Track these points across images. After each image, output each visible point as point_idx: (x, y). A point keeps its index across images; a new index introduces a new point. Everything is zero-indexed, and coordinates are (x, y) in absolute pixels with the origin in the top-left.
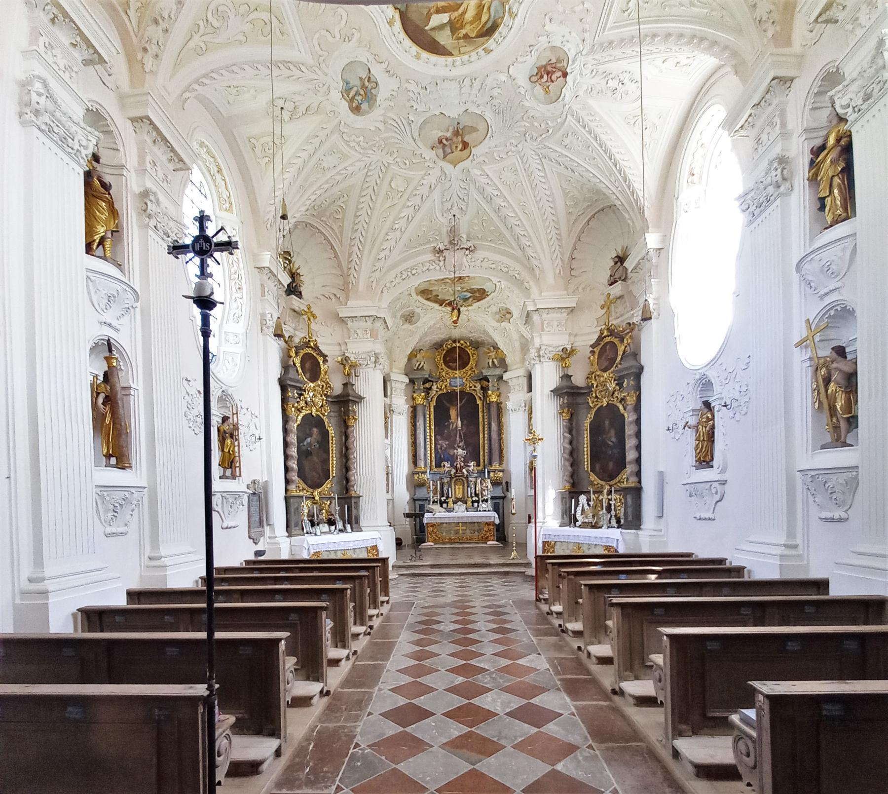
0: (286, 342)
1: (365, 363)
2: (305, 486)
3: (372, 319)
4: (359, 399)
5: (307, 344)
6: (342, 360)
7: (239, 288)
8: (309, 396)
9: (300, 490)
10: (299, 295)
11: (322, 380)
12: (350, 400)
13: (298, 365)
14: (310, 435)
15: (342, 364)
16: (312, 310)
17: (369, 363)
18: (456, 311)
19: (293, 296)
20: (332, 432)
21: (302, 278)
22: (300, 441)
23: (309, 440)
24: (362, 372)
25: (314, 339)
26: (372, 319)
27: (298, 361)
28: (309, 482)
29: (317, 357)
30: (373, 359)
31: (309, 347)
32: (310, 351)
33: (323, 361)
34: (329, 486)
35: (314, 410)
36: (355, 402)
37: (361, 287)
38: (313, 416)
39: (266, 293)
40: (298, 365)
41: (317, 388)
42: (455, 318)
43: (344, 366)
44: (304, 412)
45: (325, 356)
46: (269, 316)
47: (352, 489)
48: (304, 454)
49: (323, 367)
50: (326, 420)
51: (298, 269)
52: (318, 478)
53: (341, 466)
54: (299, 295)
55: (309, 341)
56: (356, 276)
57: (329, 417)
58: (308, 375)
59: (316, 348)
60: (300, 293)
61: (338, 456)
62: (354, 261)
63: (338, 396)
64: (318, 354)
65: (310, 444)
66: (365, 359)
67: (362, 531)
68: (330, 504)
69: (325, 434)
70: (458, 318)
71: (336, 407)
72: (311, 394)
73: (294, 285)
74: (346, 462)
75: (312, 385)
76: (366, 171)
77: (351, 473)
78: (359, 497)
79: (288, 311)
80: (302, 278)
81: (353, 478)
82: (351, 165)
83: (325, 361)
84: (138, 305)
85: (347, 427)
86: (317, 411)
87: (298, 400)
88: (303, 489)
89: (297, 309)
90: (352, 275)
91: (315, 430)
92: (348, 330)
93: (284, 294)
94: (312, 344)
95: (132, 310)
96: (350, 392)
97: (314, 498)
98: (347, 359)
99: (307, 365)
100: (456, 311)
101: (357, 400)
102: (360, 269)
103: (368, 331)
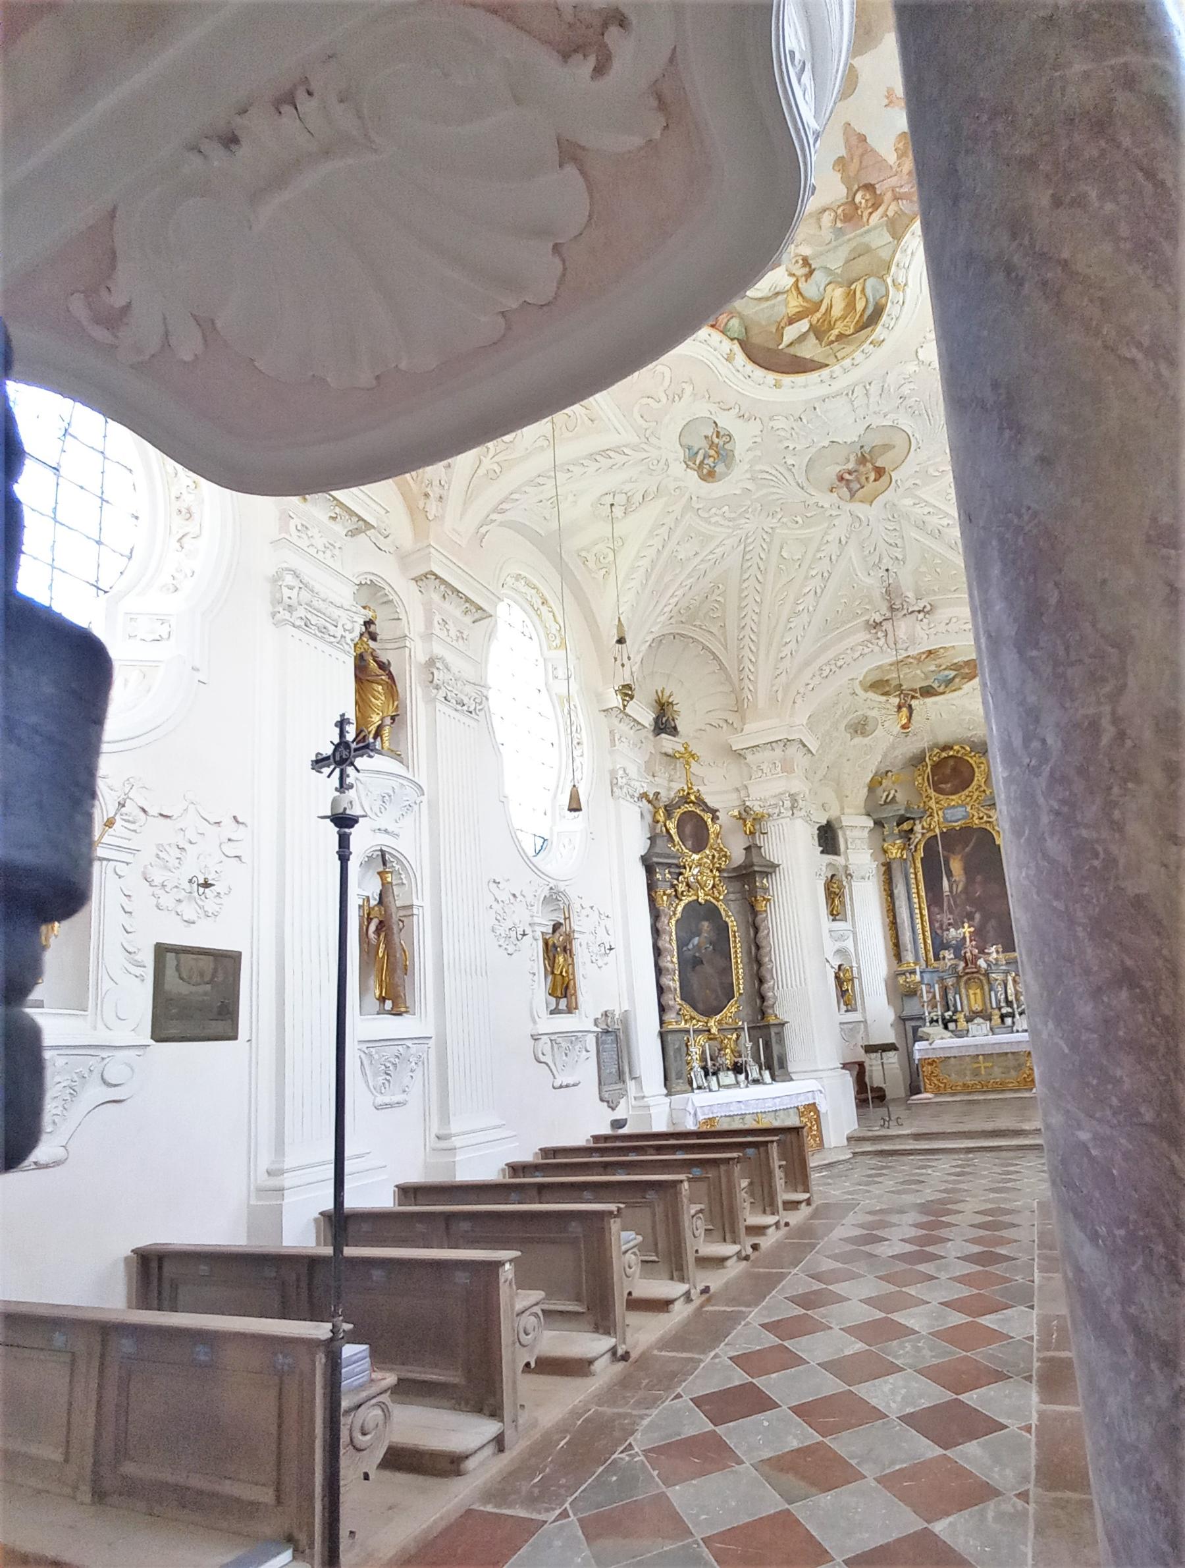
0: (649, 802)
1: (777, 811)
2: (694, 1014)
3: (781, 744)
4: (771, 869)
5: (685, 800)
6: (740, 813)
7: (578, 743)
8: (691, 874)
9: (686, 1021)
10: (674, 731)
11: (711, 848)
12: (755, 871)
13: (673, 831)
14: (699, 935)
15: (740, 818)
16: (690, 749)
17: (782, 811)
18: (904, 710)
19: (663, 735)
20: (732, 924)
21: (675, 708)
22: (682, 944)
23: (696, 940)
24: (771, 826)
25: (695, 788)
26: (781, 744)
27: (672, 826)
28: (700, 1006)
29: (702, 814)
30: (788, 804)
31: (688, 803)
32: (691, 808)
33: (712, 819)
34: (733, 1010)
35: (701, 893)
36: (766, 874)
37: (761, 703)
38: (700, 904)
39: (617, 742)
40: (673, 831)
41: (705, 860)
42: (904, 721)
43: (745, 820)
44: (686, 900)
45: (714, 812)
46: (621, 772)
47: (770, 1011)
48: (690, 964)
49: (713, 828)
50: (722, 907)
51: (670, 696)
52: (715, 999)
53: (751, 976)
54: (674, 731)
55: (688, 794)
56: (751, 688)
57: (726, 901)
58: (689, 843)
59: (700, 802)
60: (675, 728)
61: (746, 960)
62: (746, 669)
63: (734, 869)
64: (703, 810)
65: (698, 947)
66: (776, 806)
67: (792, 1080)
68: (738, 1038)
69: (722, 929)
70: (910, 718)
71: (737, 885)
72: (695, 871)
73: (664, 719)
74: (759, 969)
75: (696, 857)
76: (743, 546)
77: (766, 986)
78: (783, 1024)
79: (658, 756)
80: (675, 708)
81: (770, 994)
82: (720, 545)
83: (715, 818)
84: (424, 799)
85: (755, 913)
86: (706, 895)
87: (675, 882)
88: (692, 1018)
89: (670, 752)
90: (746, 690)
91: (705, 925)
92: (748, 765)
93: (651, 735)
94: (693, 798)
95: (416, 807)
96: (756, 860)
97: (709, 1031)
98: (747, 809)
99: (688, 829)
100: (904, 710)
101: (769, 870)
102: (756, 677)
103: (778, 764)
